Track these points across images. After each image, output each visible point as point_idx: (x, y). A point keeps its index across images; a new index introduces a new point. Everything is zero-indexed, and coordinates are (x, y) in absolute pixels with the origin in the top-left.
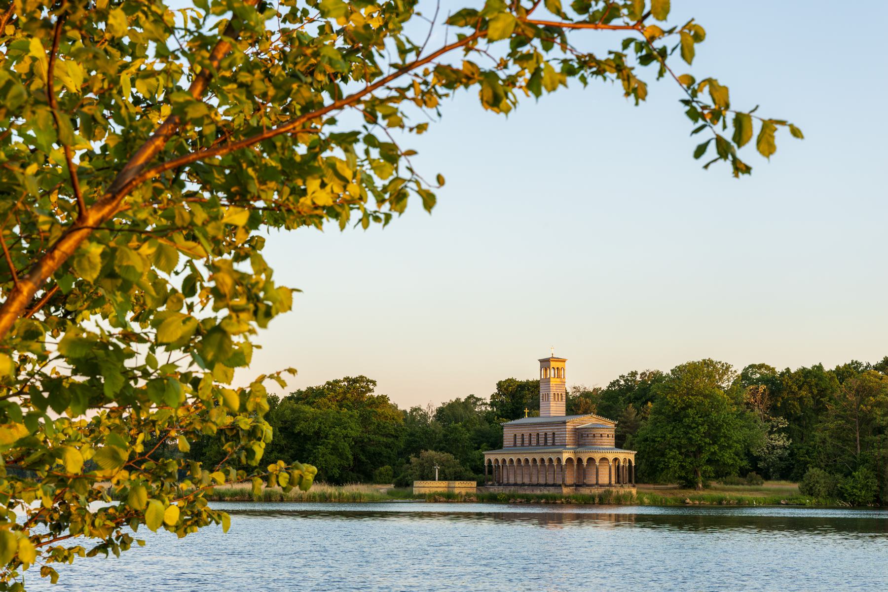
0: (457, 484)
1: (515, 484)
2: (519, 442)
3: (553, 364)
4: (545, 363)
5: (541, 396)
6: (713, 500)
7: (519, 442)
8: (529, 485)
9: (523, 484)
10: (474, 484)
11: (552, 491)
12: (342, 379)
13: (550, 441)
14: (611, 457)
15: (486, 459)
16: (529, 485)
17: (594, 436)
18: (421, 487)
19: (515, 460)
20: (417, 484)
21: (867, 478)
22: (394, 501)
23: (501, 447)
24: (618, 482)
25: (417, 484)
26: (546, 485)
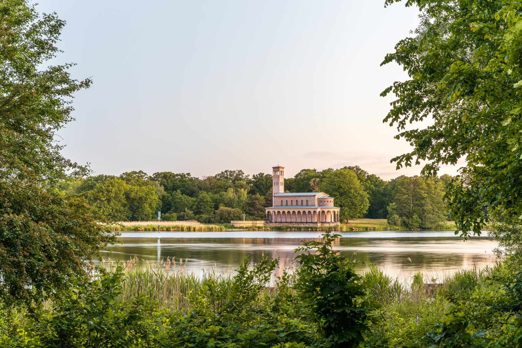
0: (258, 222)
1: (286, 222)
2: (284, 204)
3: (280, 169)
4: (276, 169)
5: (274, 183)
6: (364, 228)
7: (284, 204)
8: (296, 222)
9: (291, 222)
10: (263, 222)
11: (311, 225)
12: (138, 172)
13: (305, 203)
14: (332, 210)
15: (267, 211)
16: (296, 222)
17: (328, 202)
18: (238, 223)
19: (301, 211)
20: (232, 222)
21: (417, 218)
22: (228, 230)
23: (272, 206)
24: (335, 221)
25: (232, 222)
26: (307, 223)
